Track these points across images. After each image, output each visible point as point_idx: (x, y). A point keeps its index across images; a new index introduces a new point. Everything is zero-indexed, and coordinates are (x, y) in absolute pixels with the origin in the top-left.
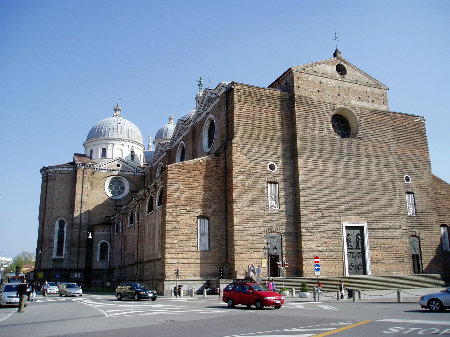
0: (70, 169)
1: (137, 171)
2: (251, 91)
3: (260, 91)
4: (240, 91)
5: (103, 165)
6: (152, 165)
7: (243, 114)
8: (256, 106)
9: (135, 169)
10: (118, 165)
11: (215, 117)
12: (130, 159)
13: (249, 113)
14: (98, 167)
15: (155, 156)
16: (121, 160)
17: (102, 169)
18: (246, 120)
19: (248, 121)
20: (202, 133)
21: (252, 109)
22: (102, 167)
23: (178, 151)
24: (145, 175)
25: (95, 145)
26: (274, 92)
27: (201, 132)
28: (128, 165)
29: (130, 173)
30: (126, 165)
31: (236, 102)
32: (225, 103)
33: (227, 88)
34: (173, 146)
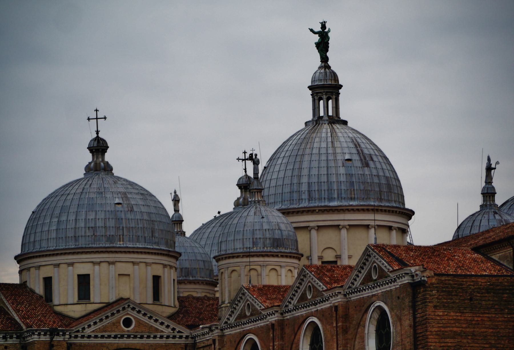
0: (10, 341)
1: (176, 333)
2: (455, 284)
3: (473, 281)
4: (437, 287)
5: (89, 326)
6: (222, 330)
7: (443, 330)
8: (465, 311)
9: (170, 330)
10: (127, 323)
11: (390, 311)
12: (150, 300)
13: (454, 325)
14: (78, 331)
15: (233, 312)
16: (133, 309)
17: (89, 337)
18: (448, 340)
19: (452, 340)
20: (364, 327)
21: (459, 318)
22: (88, 331)
23: (305, 334)
24: (195, 344)
25: (58, 265)
26: (498, 280)
27: (361, 324)
28: (152, 321)
29: (158, 341)
30: (145, 319)
31: (430, 310)
32: (410, 304)
33: (412, 276)
34: (288, 316)
